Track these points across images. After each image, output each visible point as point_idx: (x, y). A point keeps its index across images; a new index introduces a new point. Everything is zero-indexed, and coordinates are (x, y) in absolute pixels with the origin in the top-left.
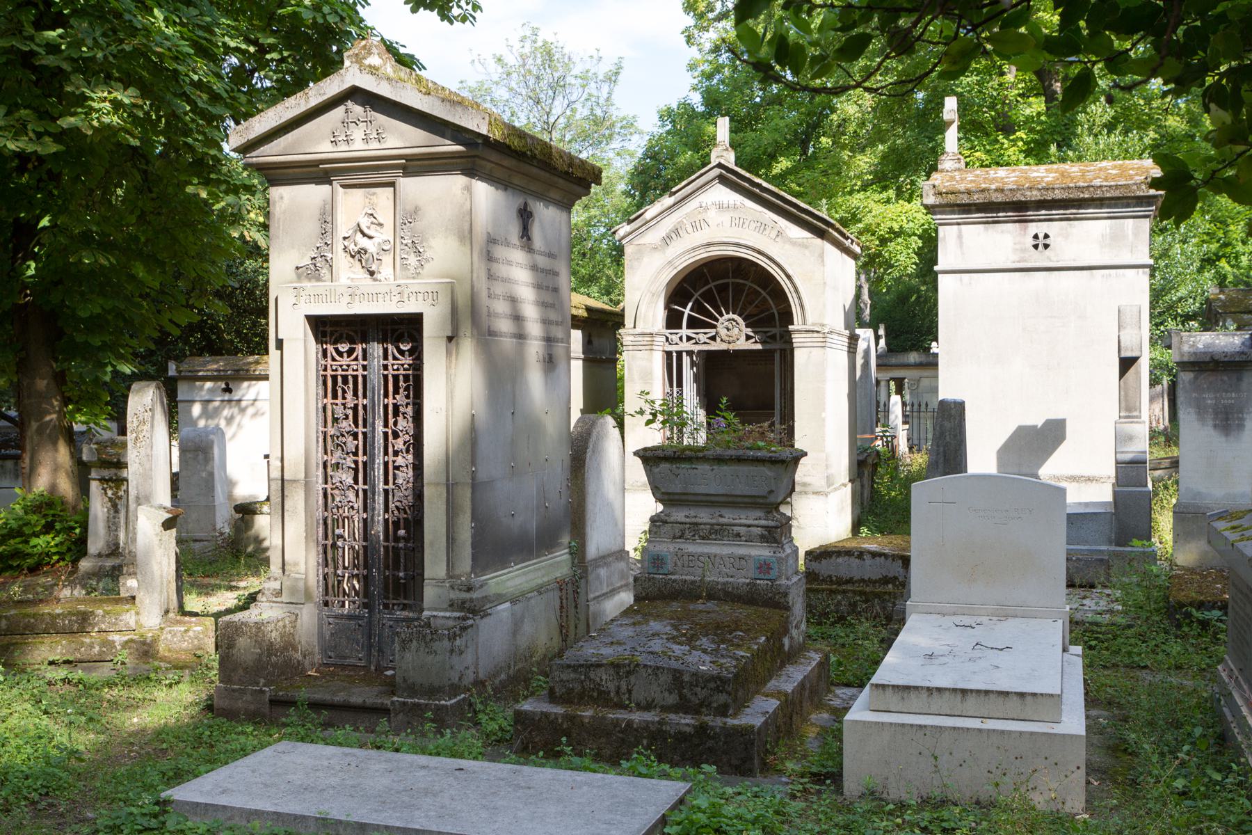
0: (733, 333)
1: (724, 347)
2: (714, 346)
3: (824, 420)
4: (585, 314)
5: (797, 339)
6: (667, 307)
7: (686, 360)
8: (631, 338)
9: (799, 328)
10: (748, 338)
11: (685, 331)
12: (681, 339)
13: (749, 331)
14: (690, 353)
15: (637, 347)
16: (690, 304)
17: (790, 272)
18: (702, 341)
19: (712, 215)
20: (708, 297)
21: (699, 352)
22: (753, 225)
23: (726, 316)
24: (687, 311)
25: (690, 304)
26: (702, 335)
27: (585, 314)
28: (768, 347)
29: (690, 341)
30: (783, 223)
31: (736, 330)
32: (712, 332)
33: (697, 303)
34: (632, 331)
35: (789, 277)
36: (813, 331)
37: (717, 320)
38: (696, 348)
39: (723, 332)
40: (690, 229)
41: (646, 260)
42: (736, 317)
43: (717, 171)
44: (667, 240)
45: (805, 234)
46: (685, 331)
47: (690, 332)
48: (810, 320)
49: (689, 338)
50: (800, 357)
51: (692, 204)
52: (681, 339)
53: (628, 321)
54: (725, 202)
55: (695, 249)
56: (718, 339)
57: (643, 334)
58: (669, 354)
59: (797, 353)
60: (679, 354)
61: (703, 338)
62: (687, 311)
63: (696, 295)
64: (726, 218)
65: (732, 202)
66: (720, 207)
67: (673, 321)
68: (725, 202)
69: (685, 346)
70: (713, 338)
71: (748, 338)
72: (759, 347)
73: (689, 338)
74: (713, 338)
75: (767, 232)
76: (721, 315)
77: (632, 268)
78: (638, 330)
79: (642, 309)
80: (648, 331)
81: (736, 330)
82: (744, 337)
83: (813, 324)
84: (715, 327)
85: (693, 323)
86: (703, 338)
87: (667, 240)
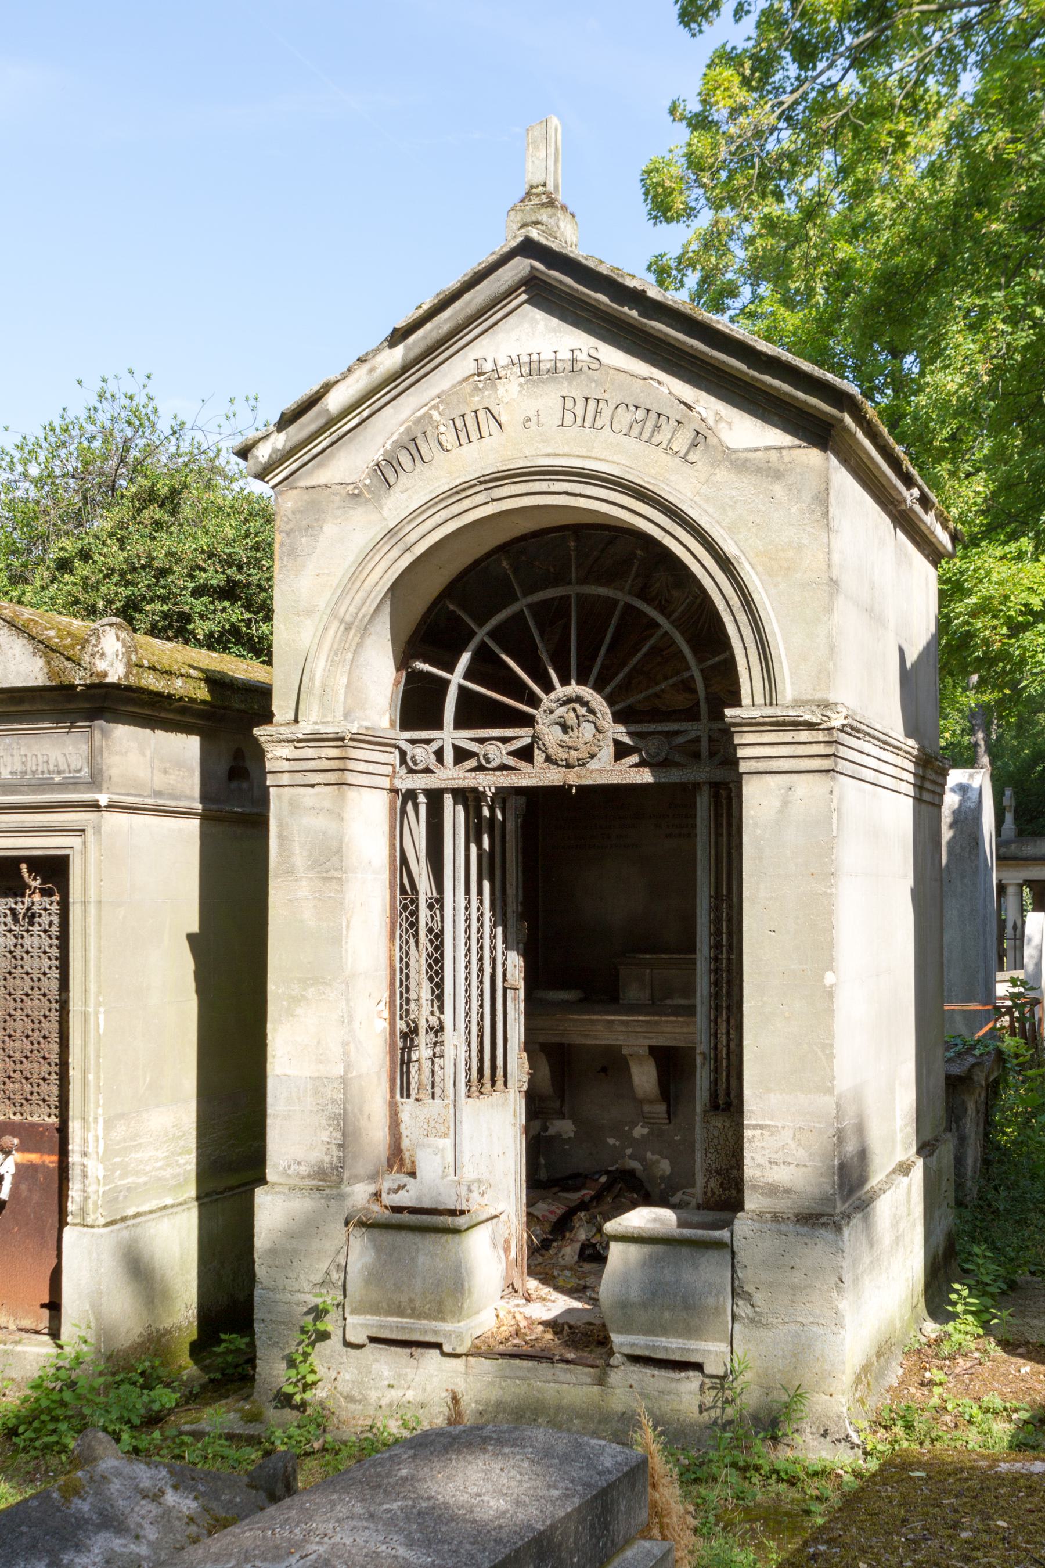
3: (830, 994)
4: (202, 693)
5: (749, 748)
6: (403, 662)
8: (287, 751)
10: (621, 751)
11: (449, 736)
12: (439, 754)
13: (620, 732)
15: (303, 777)
16: (465, 658)
17: (729, 548)
18: (496, 766)
19: (511, 396)
20: (514, 637)
21: (503, 795)
22: (624, 418)
23: (561, 691)
24: (456, 679)
25: (465, 658)
27: (202, 693)
28: (674, 776)
30: (708, 406)
31: (588, 731)
32: (523, 736)
34: (286, 732)
35: (725, 563)
36: (796, 725)
38: (487, 783)
39: (551, 735)
40: (449, 439)
41: (330, 529)
42: (586, 692)
43: (521, 266)
44: (386, 472)
45: (775, 437)
46: (449, 736)
47: (464, 738)
48: (788, 690)
49: (461, 755)
50: (759, 800)
51: (458, 367)
52: (439, 754)
53: (281, 707)
54: (547, 355)
55: (460, 491)
56: (539, 757)
57: (317, 739)
60: (435, 797)
61: (498, 754)
62: (456, 679)
63: (481, 634)
64: (547, 400)
65: (565, 355)
66: (535, 372)
67: (419, 707)
68: (547, 355)
69: (451, 775)
70: (525, 754)
71: (621, 751)
72: (645, 777)
73: (461, 755)
74: (525, 754)
75: (663, 436)
76: (549, 688)
77: (292, 552)
78: (305, 728)
80: (330, 729)
81: (588, 731)
83: (797, 704)
84: (528, 721)
86: (498, 754)
87: (386, 472)
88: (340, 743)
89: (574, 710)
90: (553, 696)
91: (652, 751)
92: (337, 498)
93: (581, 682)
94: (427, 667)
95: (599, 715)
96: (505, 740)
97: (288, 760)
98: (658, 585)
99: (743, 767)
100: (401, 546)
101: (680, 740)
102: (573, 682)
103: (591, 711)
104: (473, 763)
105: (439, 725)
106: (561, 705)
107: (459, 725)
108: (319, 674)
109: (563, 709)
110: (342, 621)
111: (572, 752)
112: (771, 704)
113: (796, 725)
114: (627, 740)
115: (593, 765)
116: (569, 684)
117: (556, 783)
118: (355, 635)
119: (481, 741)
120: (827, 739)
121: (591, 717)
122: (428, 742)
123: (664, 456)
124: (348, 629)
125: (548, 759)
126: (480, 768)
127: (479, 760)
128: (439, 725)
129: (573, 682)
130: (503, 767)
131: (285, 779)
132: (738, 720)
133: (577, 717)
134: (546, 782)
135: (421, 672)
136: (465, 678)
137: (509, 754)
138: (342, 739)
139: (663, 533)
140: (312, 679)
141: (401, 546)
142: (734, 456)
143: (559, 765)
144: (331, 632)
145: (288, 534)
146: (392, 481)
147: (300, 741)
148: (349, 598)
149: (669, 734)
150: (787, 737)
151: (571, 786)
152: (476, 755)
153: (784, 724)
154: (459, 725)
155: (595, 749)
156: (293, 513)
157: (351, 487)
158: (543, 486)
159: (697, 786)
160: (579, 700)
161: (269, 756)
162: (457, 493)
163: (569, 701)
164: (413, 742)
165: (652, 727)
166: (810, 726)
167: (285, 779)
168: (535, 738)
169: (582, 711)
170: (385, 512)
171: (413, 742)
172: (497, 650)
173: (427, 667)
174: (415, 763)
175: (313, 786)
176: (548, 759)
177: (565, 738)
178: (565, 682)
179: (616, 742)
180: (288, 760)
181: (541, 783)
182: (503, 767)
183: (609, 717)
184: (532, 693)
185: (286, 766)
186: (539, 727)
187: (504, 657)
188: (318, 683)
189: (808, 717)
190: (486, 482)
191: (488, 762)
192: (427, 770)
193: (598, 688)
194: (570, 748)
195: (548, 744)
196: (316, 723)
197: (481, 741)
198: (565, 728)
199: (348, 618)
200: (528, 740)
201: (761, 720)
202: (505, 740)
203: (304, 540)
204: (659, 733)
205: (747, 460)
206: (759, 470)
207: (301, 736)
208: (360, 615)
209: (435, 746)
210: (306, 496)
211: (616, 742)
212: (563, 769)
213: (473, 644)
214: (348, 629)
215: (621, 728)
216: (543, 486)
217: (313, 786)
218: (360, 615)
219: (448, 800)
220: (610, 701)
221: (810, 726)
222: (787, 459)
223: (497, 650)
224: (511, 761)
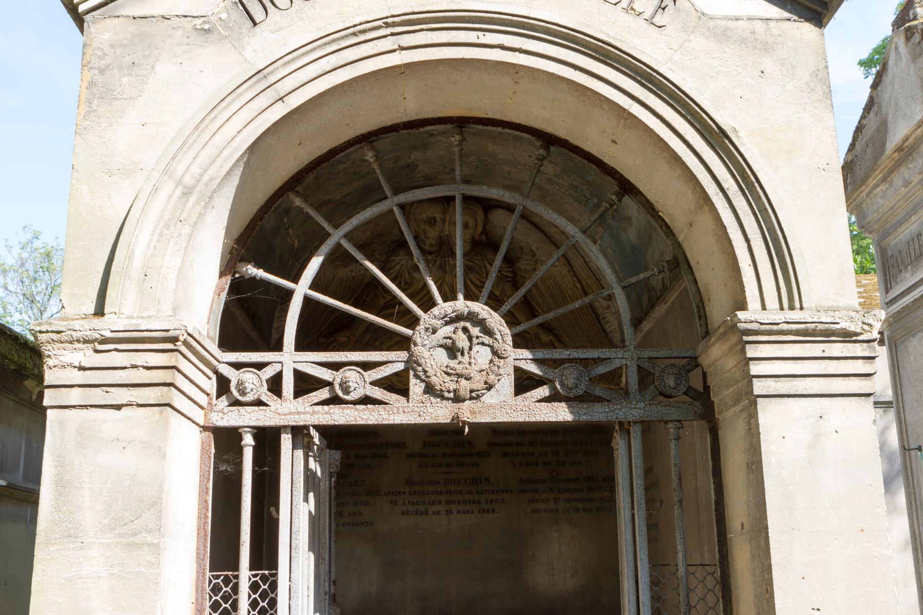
0: (468, 370)
1: (438, 413)
2: (397, 413)
5: (767, 363)
6: (229, 266)
7: (292, 464)
8: (85, 356)
9: (765, 317)
10: (524, 383)
11: (290, 359)
12: (275, 385)
13: (525, 359)
14: (299, 433)
16: (315, 264)
17: (723, 117)
18: (361, 394)
23: (444, 307)
24: (302, 289)
25: (315, 264)
26: (356, 373)
28: (598, 414)
29: (299, 394)
32: (395, 361)
33: (337, 258)
35: (717, 137)
36: (829, 334)
37: (413, 321)
39: (434, 360)
41: (165, 70)
46: (290, 359)
47: (310, 362)
49: (305, 384)
52: (275, 385)
55: (359, 32)
56: (416, 387)
58: (226, 440)
59: (769, 416)
60: (267, 439)
62: (302, 289)
63: (336, 236)
67: (249, 320)
69: (289, 410)
70: (397, 385)
71: (524, 383)
72: (561, 413)
73: (305, 384)
79: (138, 245)
81: (482, 355)
82: (507, 383)
84: (404, 343)
85: (321, 331)
86: (359, 383)
88: (169, 346)
89: (465, 330)
90: (435, 311)
91: (570, 382)
92: (180, 33)
93: (470, 296)
94: (261, 273)
95: (498, 337)
96: (366, 366)
97: (82, 368)
98: (398, 268)
99: (759, 387)
100: (271, 95)
101: (602, 369)
102: (461, 296)
103: (488, 332)
104: (324, 394)
105: (278, 346)
106: (447, 323)
107: (301, 346)
108: (139, 251)
109: (448, 330)
110: (178, 183)
111: (463, 382)
112: (792, 308)
113: (829, 334)
114: (533, 368)
115: (489, 398)
116: (455, 298)
117: (442, 420)
118: (197, 203)
119: (335, 366)
120: (867, 354)
121: (487, 339)
122: (260, 366)
123: (624, 15)
124: (187, 193)
125: (430, 389)
126: (334, 400)
127: (332, 390)
128: (278, 346)
129: (461, 296)
130: (366, 400)
131: (75, 396)
132: (755, 326)
133: (470, 338)
134: (427, 419)
135: (253, 279)
136: (311, 288)
137: (374, 383)
138: (174, 340)
139: (630, 101)
140: (130, 257)
141: (271, 95)
142: (711, 24)
143: (443, 398)
144: (162, 196)
145: (102, 71)
146: (258, 14)
147: (105, 341)
148: (192, 153)
149: (585, 363)
150: (815, 350)
151: (464, 423)
152: (330, 384)
153: (814, 333)
154: (301, 346)
155: (492, 377)
156: (112, 46)
157: (198, 22)
158: (471, 37)
159: (625, 428)
160: (472, 317)
161: (50, 362)
162: (354, 34)
163: (459, 318)
164: (237, 366)
165: (565, 354)
166: (847, 336)
167: (75, 396)
168: (412, 363)
169: (475, 331)
170: (248, 53)
171: (237, 366)
172: (358, 255)
173: (261, 273)
174: (243, 393)
175: (118, 407)
176: (430, 389)
177: (453, 363)
178: (449, 296)
179: (517, 370)
180: (82, 368)
181: (420, 421)
182: (366, 400)
183: (509, 339)
184: (408, 311)
185: (79, 377)
186: (418, 350)
187: (368, 264)
188: (137, 263)
189: (844, 325)
190: (394, 25)
191: (347, 391)
192: (259, 403)
193: (494, 303)
194: (459, 376)
195: (431, 372)
196: (132, 317)
197: (335, 366)
198: (452, 351)
199: (188, 180)
200: (400, 367)
201: (785, 327)
202: (366, 366)
203: (125, 80)
204: (571, 360)
205: (727, 29)
206: (743, 41)
207: (108, 334)
208: (206, 178)
209: (269, 372)
210: (133, 27)
211: (517, 370)
212: (449, 404)
213: (326, 248)
214: (187, 193)
215: (526, 354)
216: (471, 37)
217: (118, 407)
218: (206, 178)
219: (286, 441)
220: (511, 320)
221: (847, 336)
222: (775, 32)
223: (358, 255)
224: (377, 393)
